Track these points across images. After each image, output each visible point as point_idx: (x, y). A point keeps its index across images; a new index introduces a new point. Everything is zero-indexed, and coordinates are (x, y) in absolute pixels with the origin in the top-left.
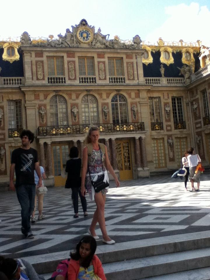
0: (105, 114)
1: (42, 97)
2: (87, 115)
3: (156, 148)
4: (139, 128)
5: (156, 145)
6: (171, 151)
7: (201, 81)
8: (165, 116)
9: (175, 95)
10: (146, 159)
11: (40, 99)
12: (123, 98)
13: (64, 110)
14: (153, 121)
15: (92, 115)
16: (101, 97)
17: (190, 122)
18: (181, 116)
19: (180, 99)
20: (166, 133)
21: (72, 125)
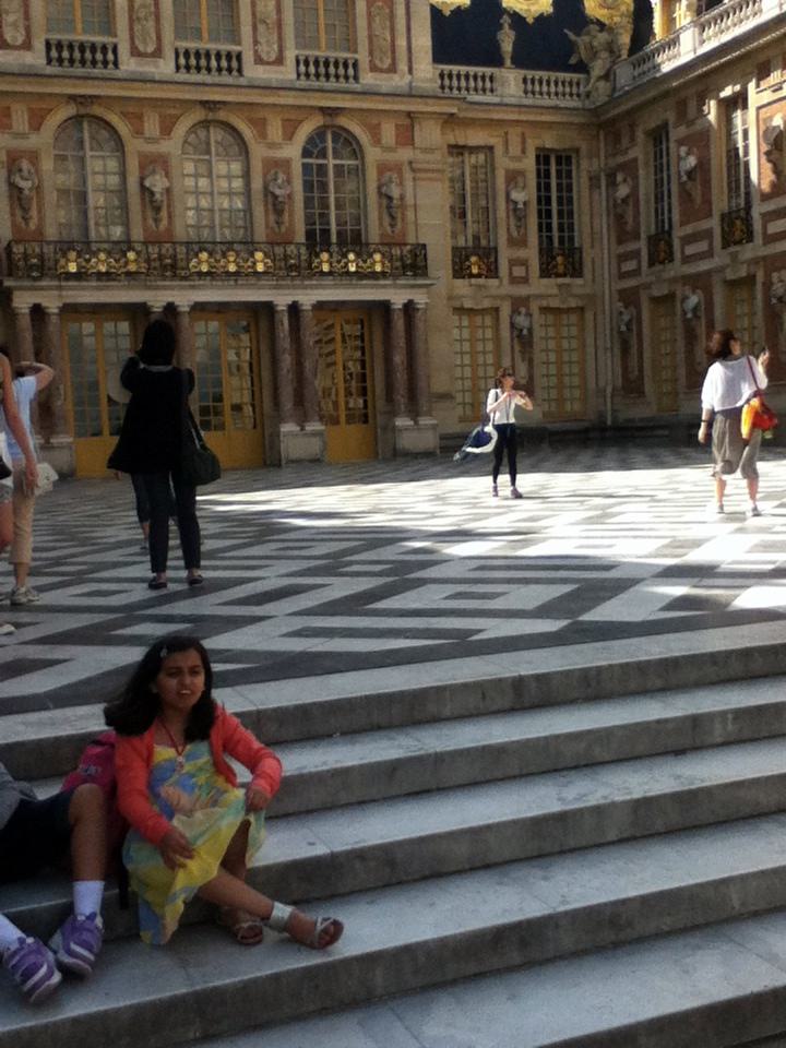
0: (277, 206)
2: (204, 203)
3: (466, 347)
4: (404, 267)
5: (466, 334)
6: (523, 360)
7: (652, 93)
8: (508, 225)
9: (549, 141)
10: (429, 386)
11: (14, 124)
12: (348, 142)
13: (114, 180)
14: (461, 242)
15: (226, 205)
17: (598, 250)
18: (567, 228)
19: (569, 162)
20: (507, 289)
21: (146, 243)
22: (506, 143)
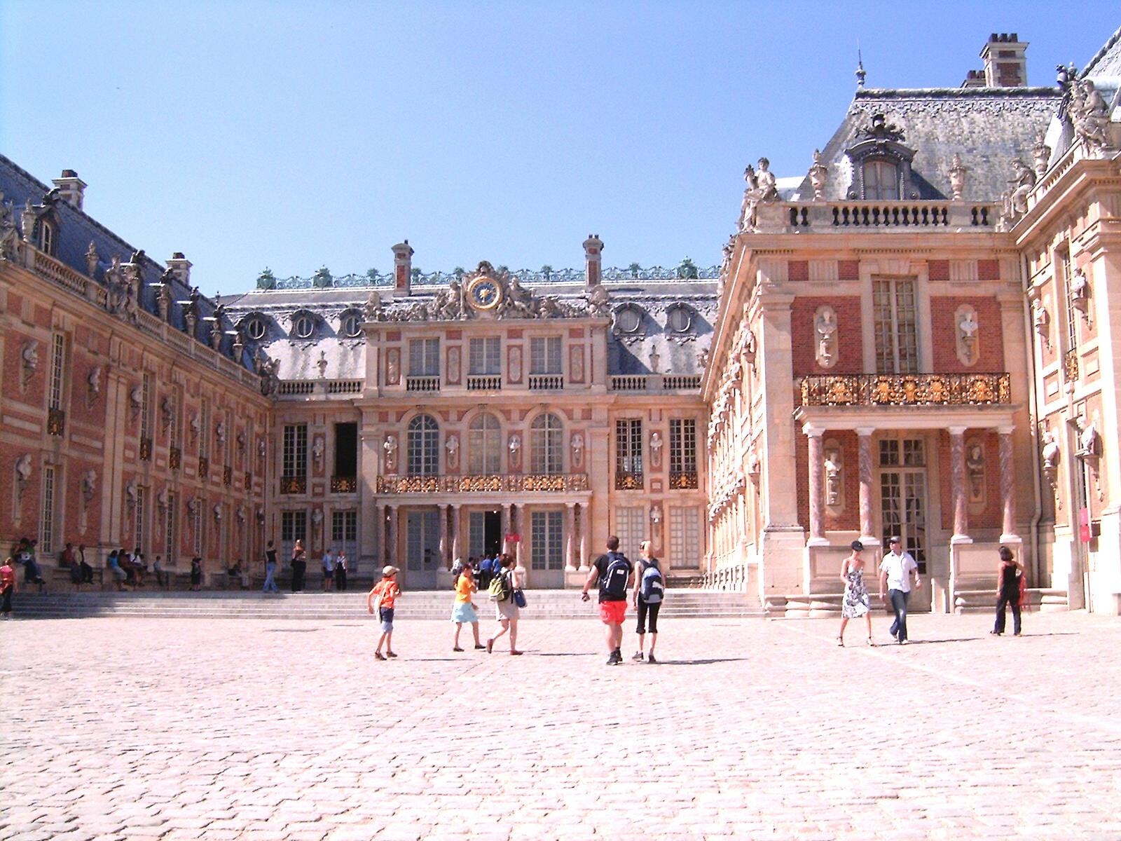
1: (392, 418)
9: (677, 414)
16: (508, 419)
22: (650, 415)
